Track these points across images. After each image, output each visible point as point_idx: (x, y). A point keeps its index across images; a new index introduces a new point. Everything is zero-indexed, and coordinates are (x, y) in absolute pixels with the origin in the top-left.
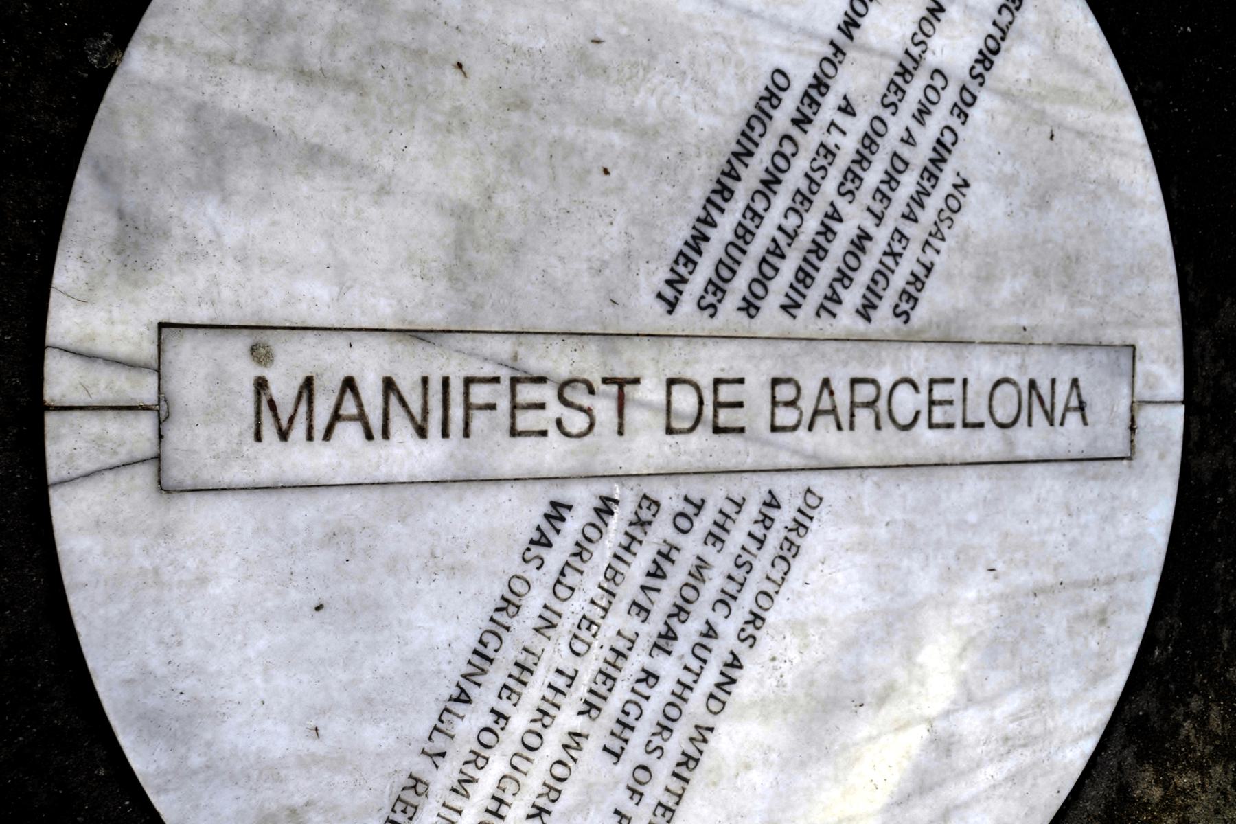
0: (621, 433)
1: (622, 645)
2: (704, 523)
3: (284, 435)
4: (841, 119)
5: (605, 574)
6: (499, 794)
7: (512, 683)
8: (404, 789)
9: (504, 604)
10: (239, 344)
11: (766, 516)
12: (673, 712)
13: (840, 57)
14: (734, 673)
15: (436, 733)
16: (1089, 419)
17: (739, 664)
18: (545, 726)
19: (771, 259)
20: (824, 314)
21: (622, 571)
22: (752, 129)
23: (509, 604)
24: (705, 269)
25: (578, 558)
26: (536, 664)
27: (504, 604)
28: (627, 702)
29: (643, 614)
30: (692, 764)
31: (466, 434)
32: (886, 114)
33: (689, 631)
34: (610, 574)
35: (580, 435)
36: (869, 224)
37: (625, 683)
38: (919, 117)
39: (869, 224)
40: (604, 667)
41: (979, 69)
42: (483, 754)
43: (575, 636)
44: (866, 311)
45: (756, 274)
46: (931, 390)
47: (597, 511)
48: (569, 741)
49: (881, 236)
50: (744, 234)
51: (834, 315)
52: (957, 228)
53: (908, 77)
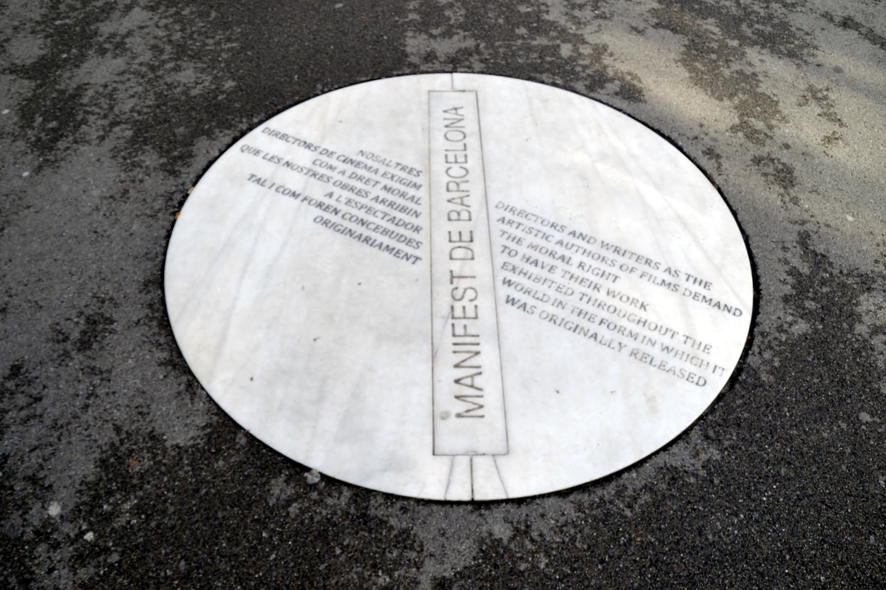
0: (474, 277)
1: (568, 276)
2: (512, 245)
3: (481, 407)
4: (335, 197)
6: (636, 321)
7: (587, 317)
9: (552, 321)
10: (441, 425)
12: (596, 256)
14: (577, 234)
16: (460, 106)
18: (605, 305)
20: (419, 202)
23: (552, 319)
24: (402, 246)
27: (552, 321)
31: (478, 336)
32: (332, 181)
33: (560, 251)
34: (537, 280)
35: (476, 292)
39: (379, 186)
41: (313, 148)
43: (565, 293)
44: (417, 186)
46: (451, 163)
47: (509, 285)
48: (611, 296)
49: (384, 182)
50: (385, 232)
51: (419, 199)
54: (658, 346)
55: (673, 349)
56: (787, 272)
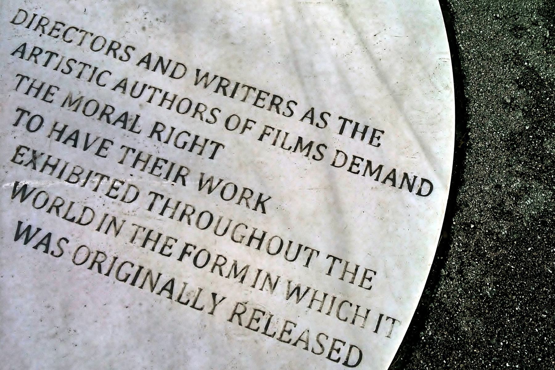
5: (73, 183)
6: (246, 240)
8: (240, 324)
11: (32, 54)
14: (154, 60)
15: (197, 305)
17: (148, 57)
18: (193, 213)
21: (72, 169)
25: (60, 208)
26: (144, 229)
28: (176, 146)
29: (107, 144)
30: (225, 83)
34: (74, 179)
37: (161, 150)
40: (148, 170)
42: (214, 261)
43: (123, 199)
48: (205, 189)
54: (282, 288)
55: (308, 289)
56: (517, 81)
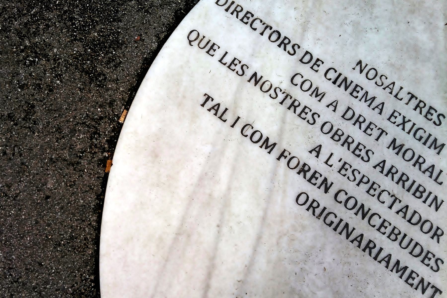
4: (324, 156)
13: (286, 154)
19: (408, 216)
22: (332, 222)
32: (319, 122)
36: (386, 140)
38: (320, 97)
39: (386, 140)
45: (418, 227)
52: (387, 73)
53: (296, 104)
